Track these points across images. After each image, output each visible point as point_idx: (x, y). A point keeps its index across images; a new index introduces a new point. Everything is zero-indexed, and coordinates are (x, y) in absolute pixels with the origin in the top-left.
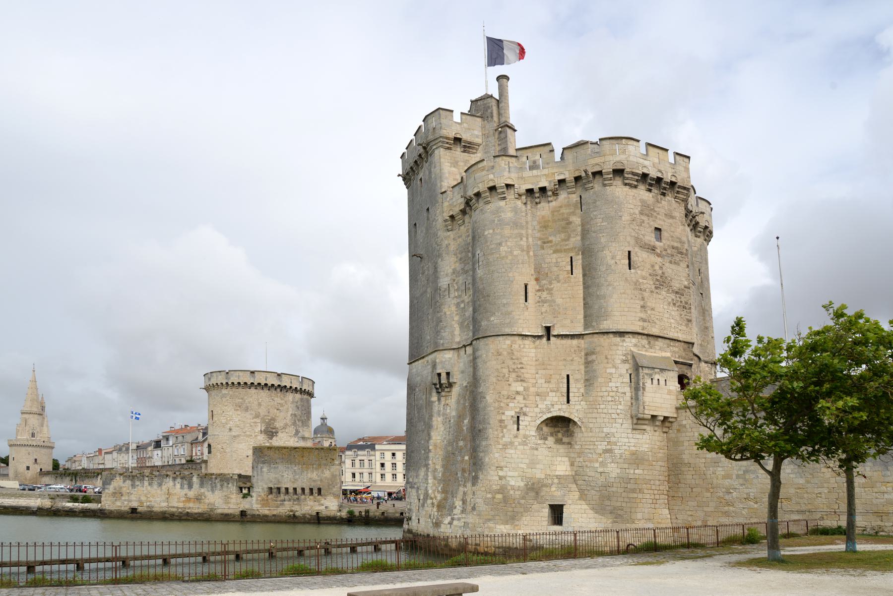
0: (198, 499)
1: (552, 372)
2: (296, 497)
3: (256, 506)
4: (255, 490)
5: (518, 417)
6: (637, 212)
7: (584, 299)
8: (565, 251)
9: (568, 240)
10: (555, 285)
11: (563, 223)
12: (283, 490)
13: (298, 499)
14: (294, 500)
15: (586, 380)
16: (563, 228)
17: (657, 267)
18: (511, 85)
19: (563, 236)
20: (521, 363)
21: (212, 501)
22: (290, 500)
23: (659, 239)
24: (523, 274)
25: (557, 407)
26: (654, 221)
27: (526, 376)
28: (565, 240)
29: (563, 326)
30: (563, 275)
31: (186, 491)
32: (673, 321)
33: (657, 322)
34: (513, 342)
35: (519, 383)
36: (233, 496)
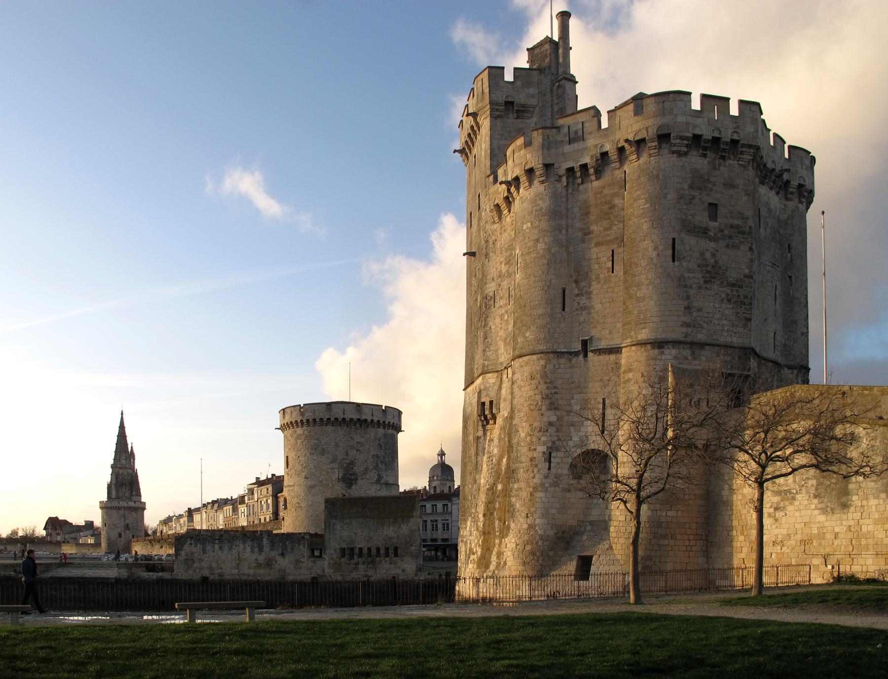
0: (269, 563)
5: (550, 453)
6: (686, 186)
9: (610, 228)
11: (606, 207)
16: (606, 214)
17: (708, 255)
19: (605, 223)
20: (555, 387)
23: (714, 217)
26: (708, 195)
27: (561, 402)
28: (606, 229)
32: (725, 322)
33: (705, 325)
35: (552, 412)
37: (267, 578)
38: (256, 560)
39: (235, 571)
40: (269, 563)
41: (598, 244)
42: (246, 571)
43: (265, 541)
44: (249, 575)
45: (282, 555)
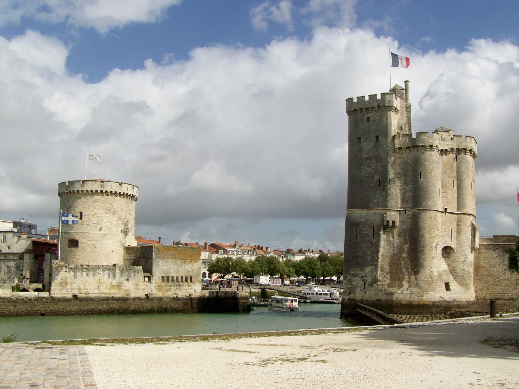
0: (119, 286)
1: (446, 227)
2: (178, 283)
3: (155, 291)
4: (154, 278)
7: (457, 199)
8: (452, 177)
10: (448, 191)
12: (170, 279)
13: (179, 285)
14: (177, 286)
15: (457, 232)
18: (409, 84)
21: (128, 287)
22: (174, 286)
24: (439, 186)
25: (448, 242)
29: (450, 209)
30: (451, 188)
31: (111, 280)
34: (436, 214)
36: (141, 284)
37: (118, 296)
38: (111, 283)
39: (97, 291)
40: (119, 286)
41: (449, 177)
42: (104, 291)
43: (117, 271)
44: (106, 293)
45: (127, 280)
